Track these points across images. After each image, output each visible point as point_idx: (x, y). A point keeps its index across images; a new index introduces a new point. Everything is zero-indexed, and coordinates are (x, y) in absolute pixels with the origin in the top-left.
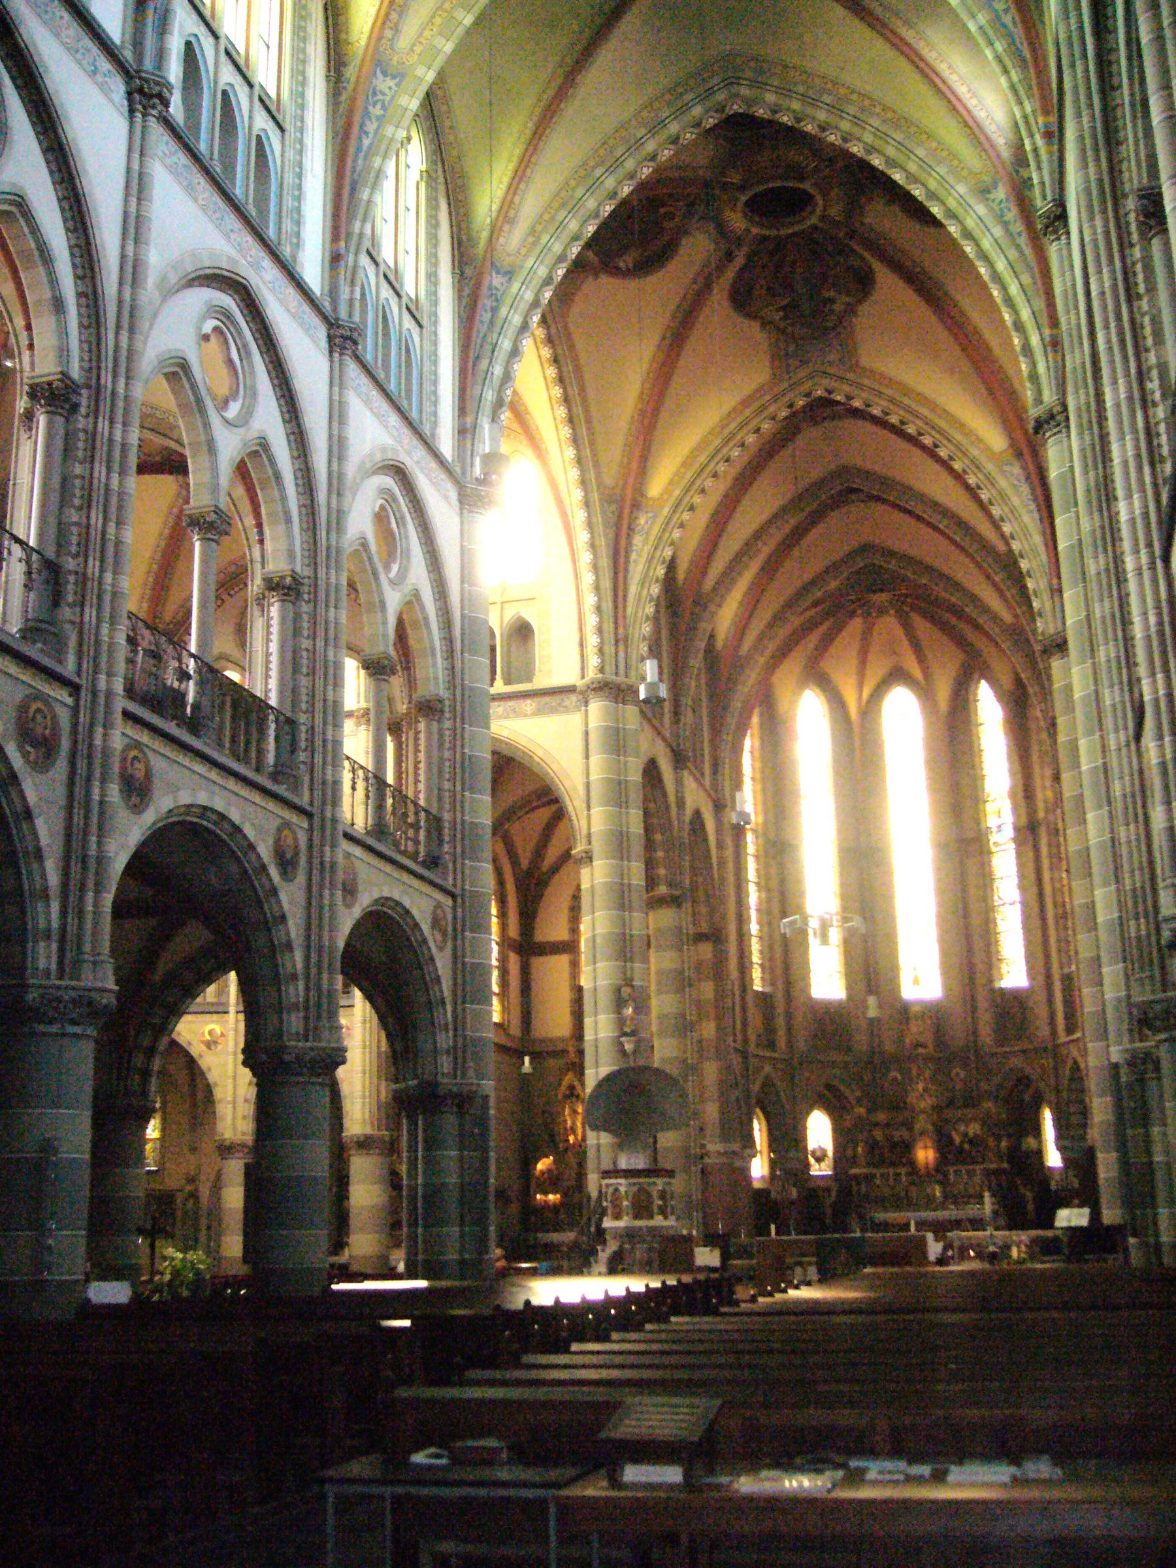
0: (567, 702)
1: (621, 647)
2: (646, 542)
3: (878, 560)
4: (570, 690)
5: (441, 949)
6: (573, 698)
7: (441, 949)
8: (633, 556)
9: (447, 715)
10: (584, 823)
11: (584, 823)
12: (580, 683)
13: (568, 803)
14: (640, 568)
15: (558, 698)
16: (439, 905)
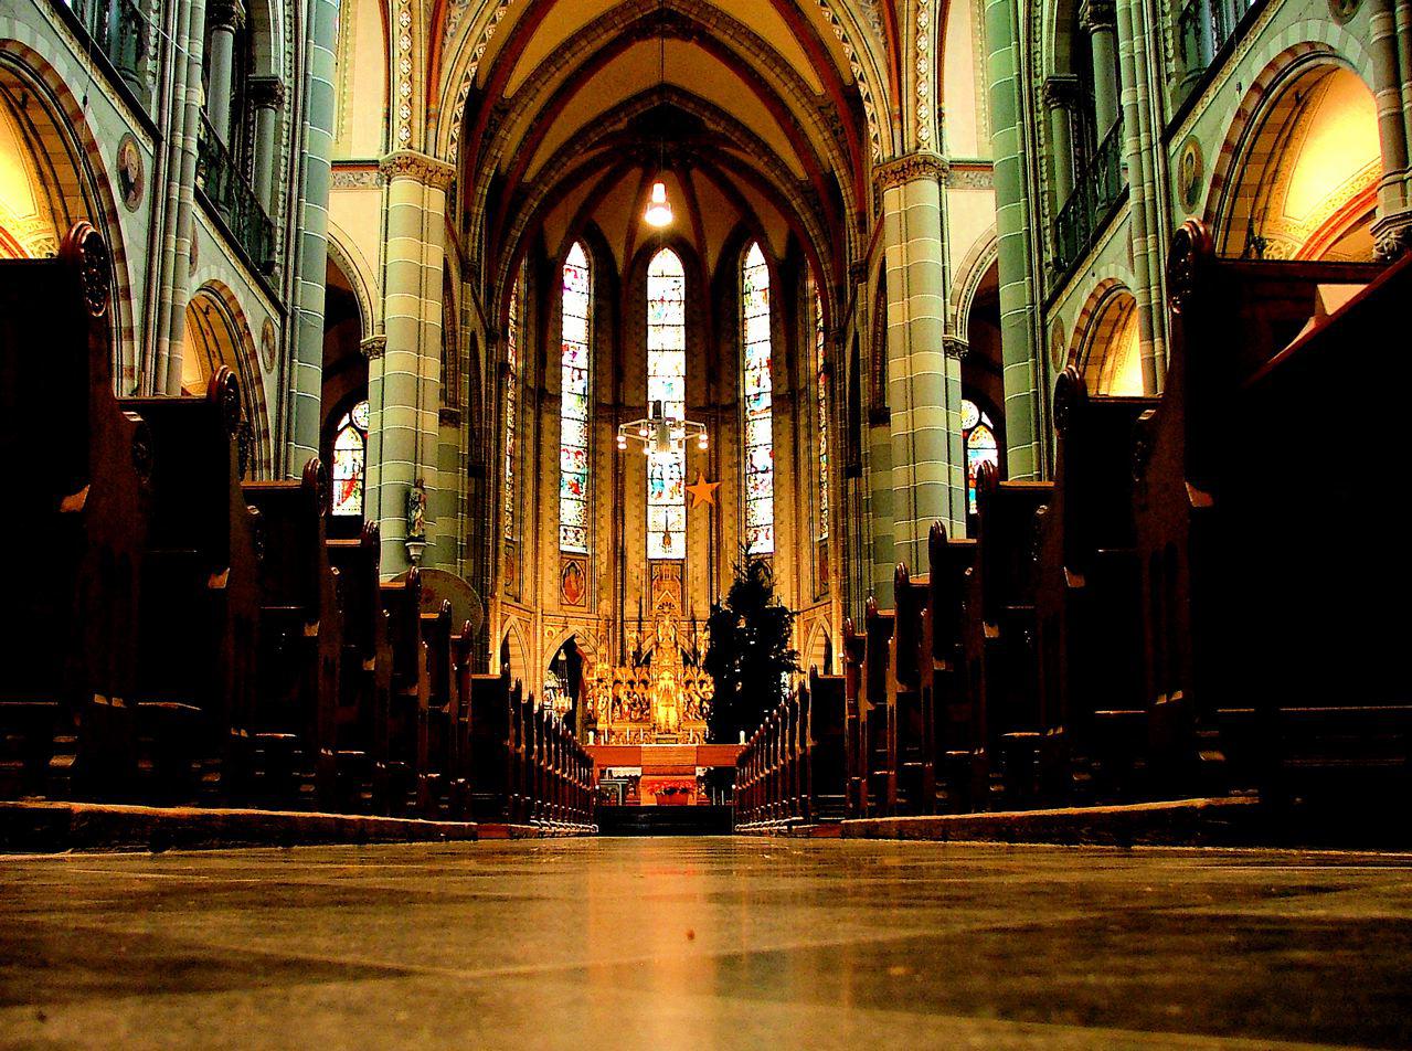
0: (366, 179)
1: (432, 123)
2: (465, 16)
3: (674, 100)
4: (374, 164)
5: (269, 371)
6: (374, 174)
7: (269, 371)
8: (451, 29)
9: (286, 106)
10: (378, 311)
11: (378, 311)
12: (382, 158)
13: (361, 287)
14: (457, 43)
15: (356, 173)
16: (268, 319)
